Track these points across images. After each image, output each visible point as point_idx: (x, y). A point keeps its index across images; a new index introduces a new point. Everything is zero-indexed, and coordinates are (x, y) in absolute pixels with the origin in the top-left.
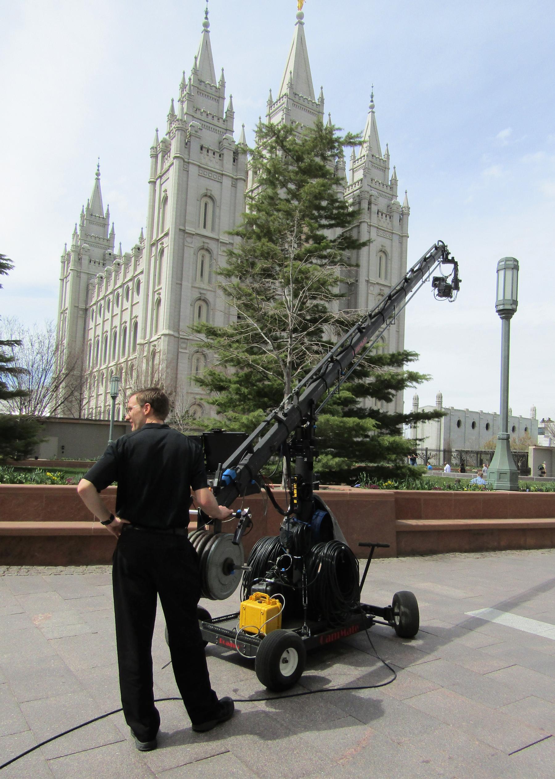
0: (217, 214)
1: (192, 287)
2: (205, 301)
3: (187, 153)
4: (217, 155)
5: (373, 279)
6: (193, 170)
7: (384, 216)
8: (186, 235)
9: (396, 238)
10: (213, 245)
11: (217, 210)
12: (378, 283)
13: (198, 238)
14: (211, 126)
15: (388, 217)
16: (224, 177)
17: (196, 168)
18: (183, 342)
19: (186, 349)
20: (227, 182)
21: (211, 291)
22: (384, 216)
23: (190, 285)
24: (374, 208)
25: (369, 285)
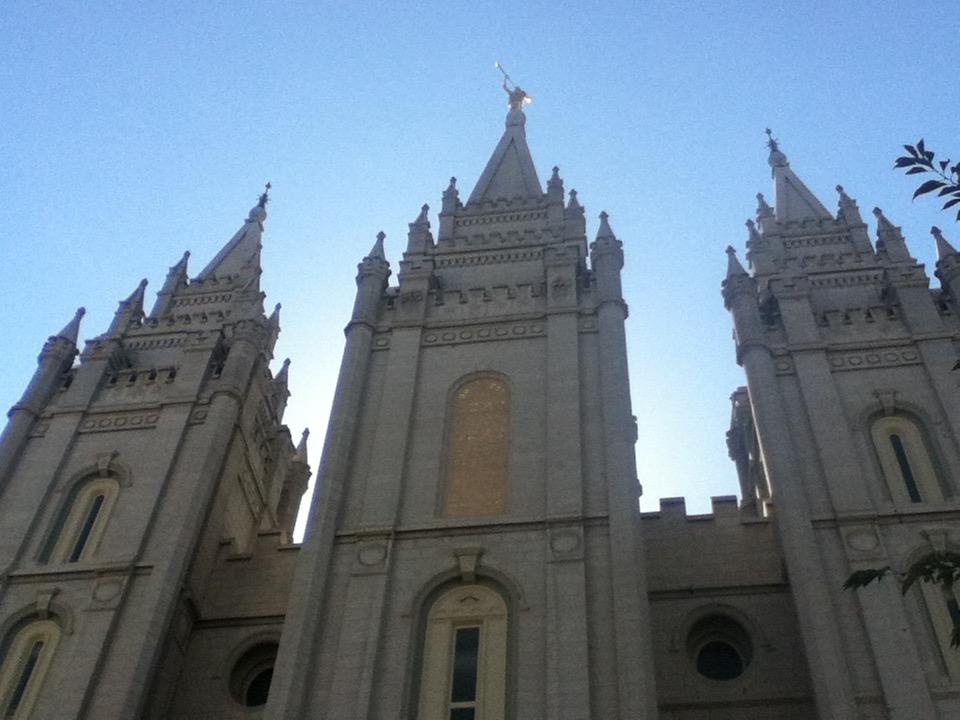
24: (796, 314)
25: (843, 530)
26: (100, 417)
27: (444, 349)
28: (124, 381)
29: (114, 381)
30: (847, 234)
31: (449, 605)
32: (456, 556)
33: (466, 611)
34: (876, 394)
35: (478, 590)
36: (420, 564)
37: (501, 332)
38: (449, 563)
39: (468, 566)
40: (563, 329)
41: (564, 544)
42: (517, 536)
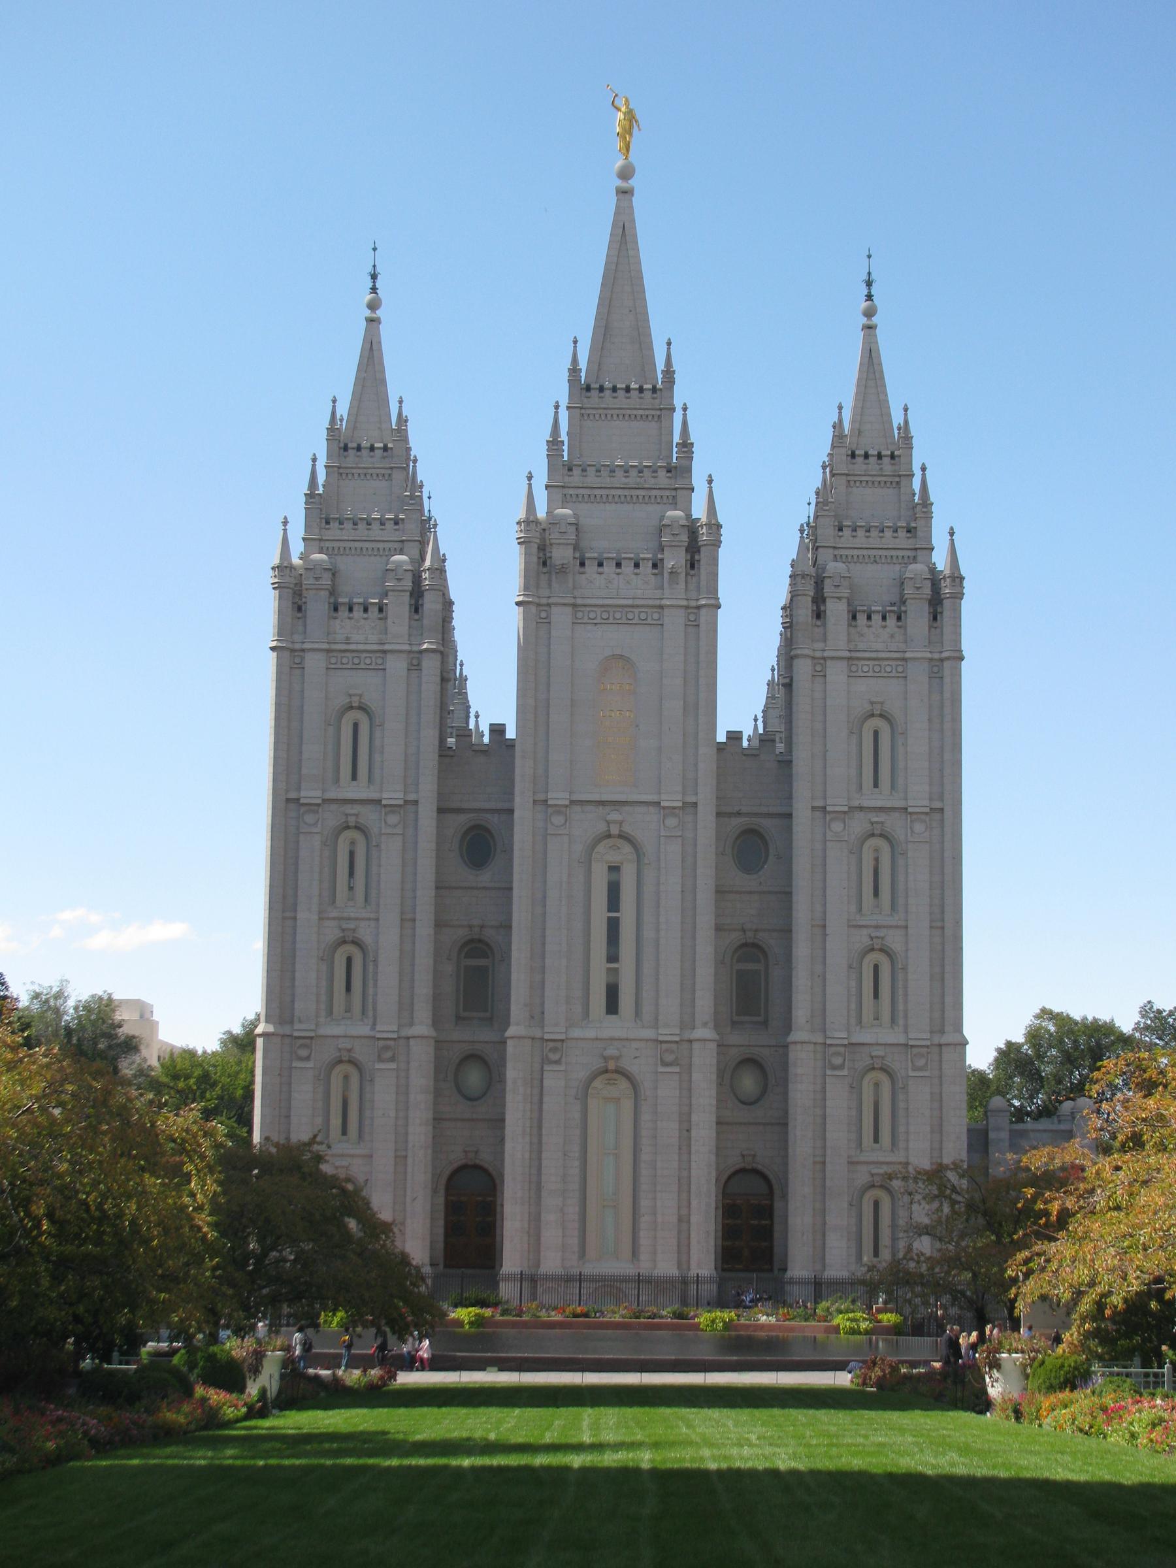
0: (377, 742)
1: (320, 919)
2: (356, 943)
3: (301, 629)
4: (374, 612)
5: (837, 802)
6: (314, 663)
7: (876, 618)
8: (303, 809)
9: (919, 674)
10: (369, 816)
11: (378, 734)
12: (861, 808)
13: (334, 807)
14: (367, 545)
15: (891, 621)
16: (389, 656)
17: (321, 656)
18: (302, 1046)
19: (308, 1058)
20: (397, 666)
21: (369, 919)
22: (876, 618)
23: (316, 917)
24: (836, 610)
25: (828, 817)
26: (339, 655)
27: (589, 627)
28: (343, 612)
29: (336, 610)
30: (897, 479)
31: (607, 854)
32: (608, 823)
33: (614, 858)
34: (872, 703)
35: (620, 842)
36: (587, 824)
37: (630, 616)
38: (602, 827)
39: (615, 830)
40: (674, 621)
41: (671, 822)
42: (644, 809)
